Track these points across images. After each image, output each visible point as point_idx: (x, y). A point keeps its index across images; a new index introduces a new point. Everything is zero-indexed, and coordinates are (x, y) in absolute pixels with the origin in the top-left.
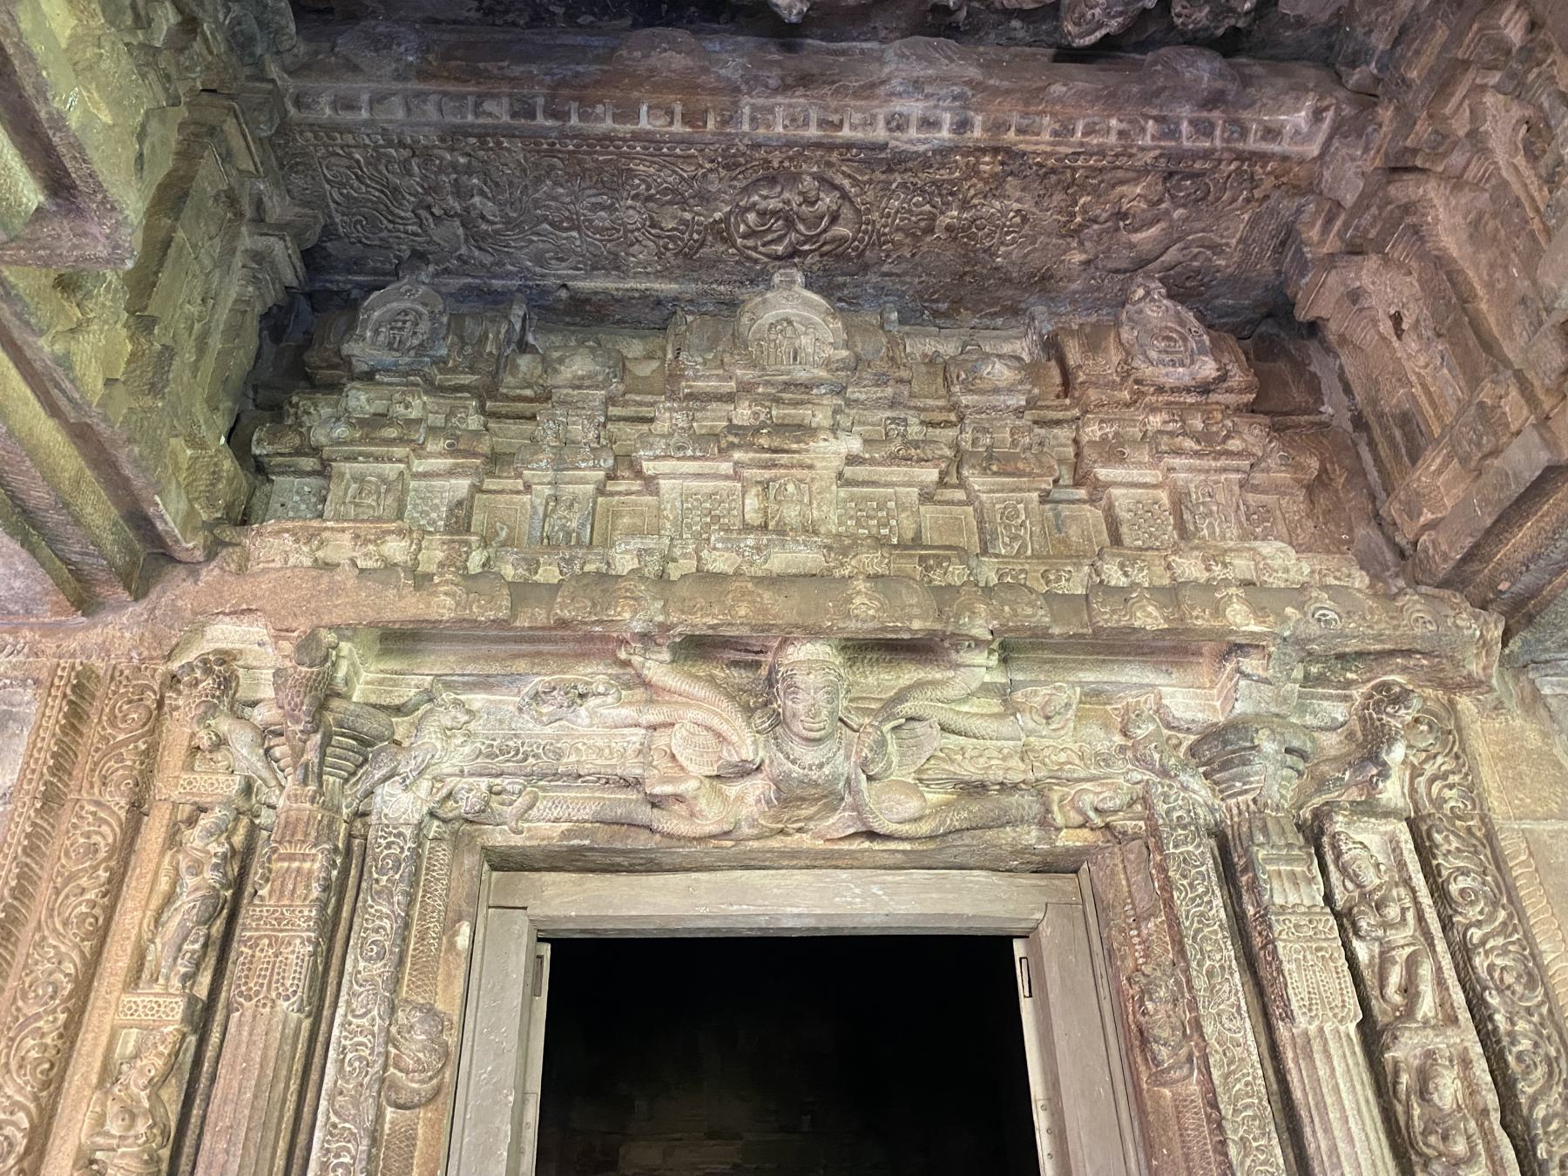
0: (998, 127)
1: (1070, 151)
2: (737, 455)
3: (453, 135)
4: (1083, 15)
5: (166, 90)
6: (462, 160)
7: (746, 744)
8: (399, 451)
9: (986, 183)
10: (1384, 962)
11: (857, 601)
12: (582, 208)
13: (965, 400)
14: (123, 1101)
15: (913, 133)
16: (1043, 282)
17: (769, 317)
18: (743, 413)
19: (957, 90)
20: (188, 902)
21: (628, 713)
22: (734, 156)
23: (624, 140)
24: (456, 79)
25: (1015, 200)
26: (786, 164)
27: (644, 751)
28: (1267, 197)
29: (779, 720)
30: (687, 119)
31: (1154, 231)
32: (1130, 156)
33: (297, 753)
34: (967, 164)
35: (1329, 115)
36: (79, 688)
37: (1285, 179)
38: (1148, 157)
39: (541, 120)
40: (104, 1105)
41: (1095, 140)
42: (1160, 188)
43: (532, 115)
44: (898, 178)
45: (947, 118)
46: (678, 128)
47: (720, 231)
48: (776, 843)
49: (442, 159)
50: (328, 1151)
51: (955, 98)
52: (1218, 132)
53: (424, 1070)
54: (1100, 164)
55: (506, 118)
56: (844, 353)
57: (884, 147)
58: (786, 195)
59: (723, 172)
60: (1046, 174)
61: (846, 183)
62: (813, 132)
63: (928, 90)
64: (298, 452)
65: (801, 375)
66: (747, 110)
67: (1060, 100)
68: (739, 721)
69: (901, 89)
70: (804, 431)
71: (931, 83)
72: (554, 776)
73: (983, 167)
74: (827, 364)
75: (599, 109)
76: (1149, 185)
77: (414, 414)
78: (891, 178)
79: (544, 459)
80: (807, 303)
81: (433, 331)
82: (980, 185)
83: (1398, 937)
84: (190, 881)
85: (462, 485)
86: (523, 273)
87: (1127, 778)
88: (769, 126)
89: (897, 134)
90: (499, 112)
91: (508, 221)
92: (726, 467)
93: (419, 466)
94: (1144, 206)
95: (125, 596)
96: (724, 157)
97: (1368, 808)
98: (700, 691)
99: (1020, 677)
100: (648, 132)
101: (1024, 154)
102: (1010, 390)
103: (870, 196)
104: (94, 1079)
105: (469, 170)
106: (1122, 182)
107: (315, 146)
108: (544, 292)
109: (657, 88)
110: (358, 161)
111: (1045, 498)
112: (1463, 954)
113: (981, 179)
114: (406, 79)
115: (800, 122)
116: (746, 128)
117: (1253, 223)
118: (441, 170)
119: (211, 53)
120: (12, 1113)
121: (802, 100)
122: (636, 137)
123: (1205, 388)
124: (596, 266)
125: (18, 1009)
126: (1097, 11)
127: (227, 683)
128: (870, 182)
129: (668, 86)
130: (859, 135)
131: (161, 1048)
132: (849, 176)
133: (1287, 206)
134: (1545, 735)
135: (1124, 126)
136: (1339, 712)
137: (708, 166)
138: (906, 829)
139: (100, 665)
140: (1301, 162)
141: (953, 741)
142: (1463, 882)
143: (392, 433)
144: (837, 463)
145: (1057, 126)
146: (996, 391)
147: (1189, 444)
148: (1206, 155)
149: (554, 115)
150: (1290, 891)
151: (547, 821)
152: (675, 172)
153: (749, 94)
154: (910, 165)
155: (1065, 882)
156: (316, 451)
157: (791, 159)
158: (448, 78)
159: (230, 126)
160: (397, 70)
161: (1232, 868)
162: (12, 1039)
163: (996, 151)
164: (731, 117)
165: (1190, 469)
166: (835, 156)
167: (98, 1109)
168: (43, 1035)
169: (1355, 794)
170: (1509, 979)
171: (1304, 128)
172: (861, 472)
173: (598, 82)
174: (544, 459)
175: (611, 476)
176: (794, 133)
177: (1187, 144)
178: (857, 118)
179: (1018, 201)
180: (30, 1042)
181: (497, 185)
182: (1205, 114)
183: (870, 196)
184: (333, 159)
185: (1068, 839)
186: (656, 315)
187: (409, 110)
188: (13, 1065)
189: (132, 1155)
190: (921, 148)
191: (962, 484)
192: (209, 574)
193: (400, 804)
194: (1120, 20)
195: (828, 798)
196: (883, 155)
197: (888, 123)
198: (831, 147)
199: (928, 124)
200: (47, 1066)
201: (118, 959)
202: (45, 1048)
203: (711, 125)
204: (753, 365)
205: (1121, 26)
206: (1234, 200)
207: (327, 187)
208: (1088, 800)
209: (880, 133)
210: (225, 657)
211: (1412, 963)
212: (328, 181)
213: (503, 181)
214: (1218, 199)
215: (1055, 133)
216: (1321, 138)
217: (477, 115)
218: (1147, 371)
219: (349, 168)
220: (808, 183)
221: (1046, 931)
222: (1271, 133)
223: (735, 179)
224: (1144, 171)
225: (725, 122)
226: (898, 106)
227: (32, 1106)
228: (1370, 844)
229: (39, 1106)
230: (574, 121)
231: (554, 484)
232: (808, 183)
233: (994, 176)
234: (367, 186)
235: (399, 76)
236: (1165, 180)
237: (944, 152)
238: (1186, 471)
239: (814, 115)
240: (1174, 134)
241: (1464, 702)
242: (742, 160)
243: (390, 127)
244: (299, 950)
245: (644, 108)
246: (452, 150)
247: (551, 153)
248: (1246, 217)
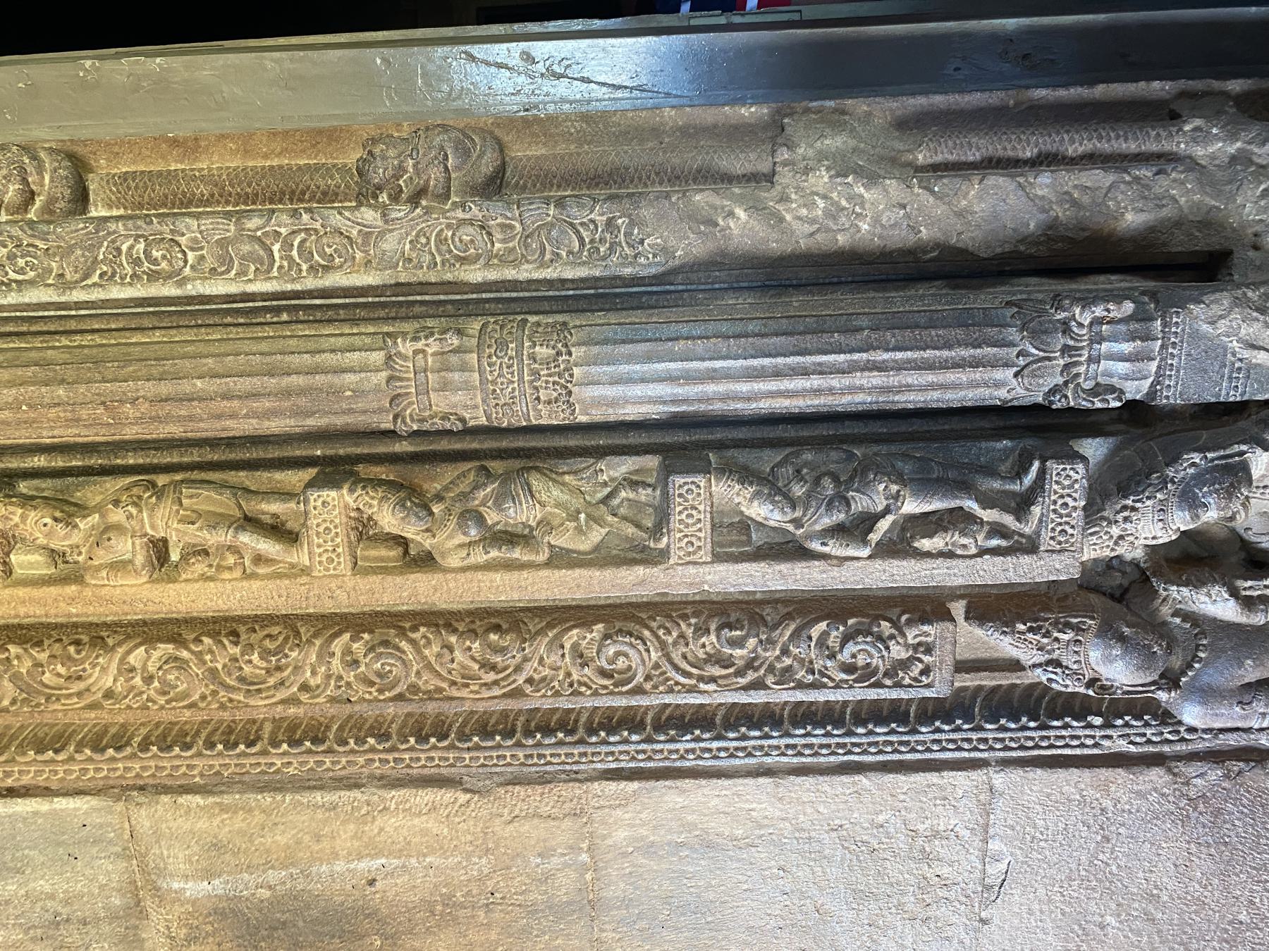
14: (91, 546)
40: (98, 569)
50: (134, 276)
53: (23, 170)
104: (72, 589)
120: (132, 670)
125: (14, 702)
131: (16, 519)
162: (48, 698)
167: (104, 573)
168: (38, 665)
180: (47, 678)
188: (81, 685)
189: (150, 517)
200: (72, 649)
202: (53, 656)
227: (121, 650)
229: (120, 644)
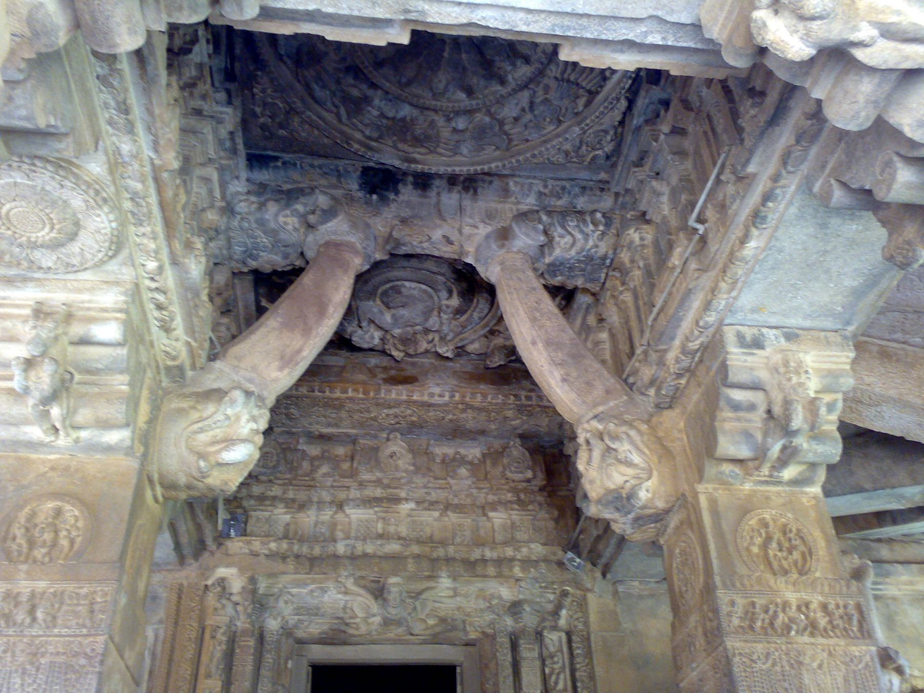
0: (464, 396)
2: (376, 509)
7: (375, 607)
8: (269, 508)
10: (551, 673)
11: (409, 566)
12: (327, 414)
13: (452, 482)
16: (483, 432)
17: (388, 452)
18: (379, 492)
20: (218, 655)
21: (340, 596)
25: (470, 414)
27: (344, 608)
29: (385, 600)
31: (518, 422)
33: (246, 609)
36: (179, 589)
39: (317, 393)
43: (313, 391)
45: (447, 394)
46: (361, 396)
47: (375, 419)
48: (382, 637)
55: (305, 392)
56: (412, 468)
62: (404, 397)
64: (237, 508)
65: (398, 475)
68: (373, 601)
70: (397, 500)
72: (315, 612)
74: (406, 471)
77: (272, 494)
79: (315, 507)
80: (402, 447)
81: (278, 461)
83: (556, 666)
84: (219, 648)
85: (288, 517)
86: (304, 427)
87: (489, 617)
91: (301, 416)
92: (371, 511)
93: (276, 511)
95: (193, 561)
97: (555, 628)
98: (362, 592)
99: (458, 585)
102: (467, 478)
108: (310, 432)
111: (474, 520)
112: (573, 671)
116: (383, 396)
117: (550, 421)
122: (347, 398)
123: (528, 481)
124: (329, 425)
127: (224, 588)
130: (419, 398)
134: (615, 605)
136: (552, 597)
138: (422, 632)
139: (185, 583)
141: (437, 605)
142: (578, 651)
143: (268, 503)
144: (407, 512)
146: (462, 479)
147: (516, 506)
148: (530, 406)
150: (529, 653)
151: (315, 628)
155: (470, 648)
156: (244, 508)
161: (514, 647)
165: (517, 515)
169: (553, 624)
170: (584, 679)
172: (414, 513)
174: (315, 507)
175: (335, 513)
178: (419, 394)
182: (529, 394)
185: (473, 636)
186: (349, 440)
191: (447, 516)
192: (218, 555)
193: (273, 624)
195: (398, 623)
199: (441, 396)
201: (202, 670)
204: (382, 471)
208: (477, 624)
209: (426, 398)
210: (222, 582)
211: (558, 674)
218: (509, 475)
221: (465, 665)
228: (554, 639)
230: (327, 393)
231: (317, 516)
237: (446, 405)
238: (516, 515)
240: (520, 400)
241: (590, 596)
244: (249, 668)
245: (350, 390)
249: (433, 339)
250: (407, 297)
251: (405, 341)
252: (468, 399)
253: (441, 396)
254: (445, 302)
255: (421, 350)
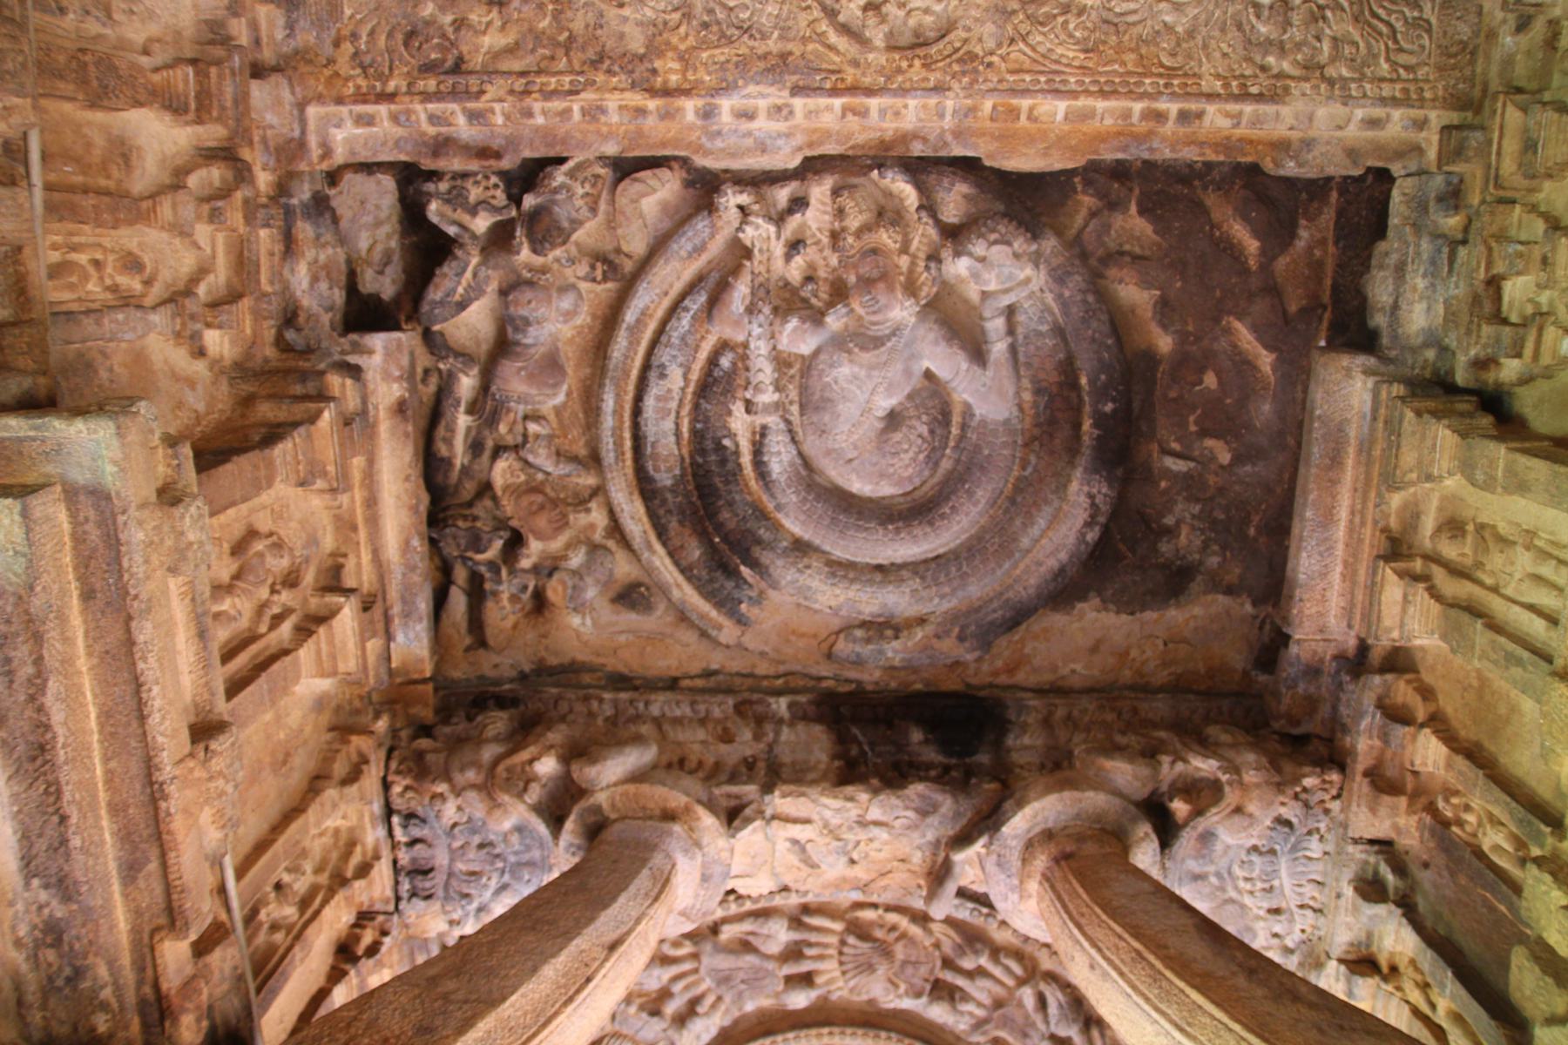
1: (583, 95)
3: (1274, 96)
4: (594, 186)
5: (1554, 249)
6: (1271, 60)
9: (668, 43)
15: (762, 104)
19: (719, 144)
22: (964, 73)
23: (1087, 92)
24: (1251, 142)
26: (904, 64)
28: (337, 44)
30: (1014, 113)
32: (512, 92)
34: (695, 70)
35: (315, 152)
37: (327, 72)
38: (492, 91)
41: (557, 105)
42: (464, 49)
43: (1184, 116)
44: (773, 45)
45: (725, 117)
49: (1296, 63)
51: (719, 133)
52: (423, 117)
54: (544, 79)
55: (1211, 109)
57: (797, 90)
58: (901, 13)
59: (978, 50)
60: (601, 60)
61: (833, 38)
62: (874, 103)
63: (749, 142)
66: (948, 118)
67: (605, 138)
69: (780, 142)
71: (749, 150)
73: (676, 66)
75: (1108, 122)
76: (477, 51)
78: (780, 45)
82: (675, 40)
88: (925, 107)
89: (780, 102)
90: (1216, 119)
94: (473, 17)
96: (975, 71)
100: (1061, 99)
101: (633, 86)
103: (803, 19)
105: (1267, 45)
106: (512, 50)
107: (1427, 81)
109: (1044, 134)
110: (1388, 59)
113: (675, 49)
114: (1302, 141)
115: (889, 112)
118: (1298, 46)
119: (1490, 249)
121: (885, 125)
122: (1074, 95)
126: (580, 191)
128: (804, 40)
129: (1030, 139)
130: (823, 101)
132: (831, 48)
133: (306, 36)
135: (531, 122)
137: (995, 59)
140: (320, 99)
145: (603, 119)
148: (427, 97)
149: (1160, 117)
152: (1034, 49)
153: (943, 131)
154: (762, 65)
157: (899, 71)
158: (1259, 142)
159: (1508, 166)
160: (1309, 151)
163: (667, 92)
164: (966, 116)
166: (850, 75)
171: (333, 131)
173: (1103, 140)
176: (899, 102)
177: (454, 106)
179: (626, 19)
181: (1239, 27)
182: (443, 130)
183: (803, 19)
184: (1413, 60)
187: (1311, 118)
190: (752, 89)
194: (555, 184)
196: (794, 78)
197: (791, 113)
198: (854, 89)
199: (749, 115)
203: (988, 105)
205: (550, 176)
206: (372, 33)
207: (1434, 21)
209: (798, 103)
212: (1429, 31)
213: (1233, 33)
214: (390, 35)
215: (603, 110)
216: (312, 126)
217: (1241, 113)
219: (1401, 50)
220: (878, 36)
222: (367, 121)
223: (966, 41)
224: (490, 73)
225: (973, 110)
226: (781, 126)
232: (878, 36)
233: (661, 54)
234: (1388, 24)
235: (1308, 144)
236: (460, 60)
239: (874, 114)
242: (956, 67)
243: (1338, 105)
246: (1281, 75)
247: (1171, 72)
248: (348, 12)
249: (788, 257)
250: (882, 475)
251: (877, 279)
252: (652, 104)
253: (749, 115)
254: (772, 420)
255: (820, 191)
